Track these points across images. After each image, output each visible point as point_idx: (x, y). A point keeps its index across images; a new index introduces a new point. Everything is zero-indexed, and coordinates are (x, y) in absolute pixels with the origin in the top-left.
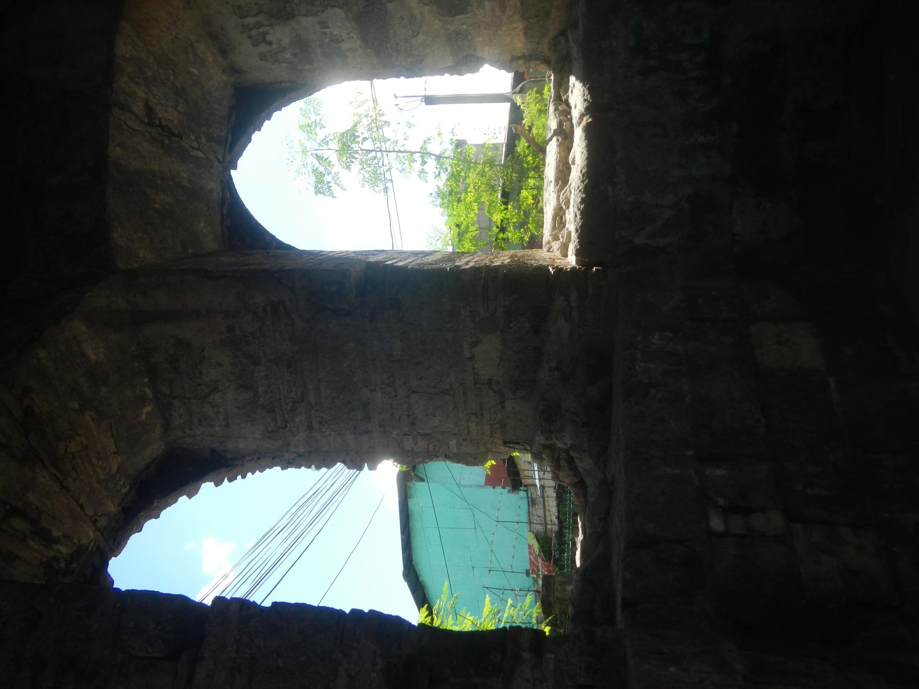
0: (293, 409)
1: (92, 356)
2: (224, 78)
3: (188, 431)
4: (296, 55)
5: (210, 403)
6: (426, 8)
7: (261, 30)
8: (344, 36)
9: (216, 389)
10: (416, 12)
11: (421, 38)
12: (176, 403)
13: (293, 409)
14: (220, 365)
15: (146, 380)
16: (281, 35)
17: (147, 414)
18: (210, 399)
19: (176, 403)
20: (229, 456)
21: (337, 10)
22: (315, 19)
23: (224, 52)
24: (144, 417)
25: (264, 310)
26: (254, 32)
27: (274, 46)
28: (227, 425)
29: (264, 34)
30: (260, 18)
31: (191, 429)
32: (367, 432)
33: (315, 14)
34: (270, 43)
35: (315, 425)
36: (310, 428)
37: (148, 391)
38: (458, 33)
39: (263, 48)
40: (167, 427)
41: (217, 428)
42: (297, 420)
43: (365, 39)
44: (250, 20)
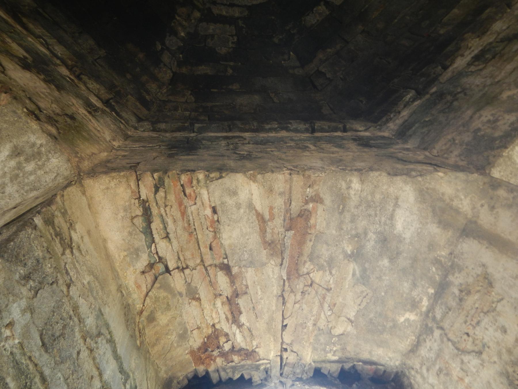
3: (424, 371)
5: (462, 362)
14: (504, 331)
15: (431, 291)
17: (408, 320)
18: (466, 358)
19: (437, 333)
24: (402, 319)
31: (428, 370)
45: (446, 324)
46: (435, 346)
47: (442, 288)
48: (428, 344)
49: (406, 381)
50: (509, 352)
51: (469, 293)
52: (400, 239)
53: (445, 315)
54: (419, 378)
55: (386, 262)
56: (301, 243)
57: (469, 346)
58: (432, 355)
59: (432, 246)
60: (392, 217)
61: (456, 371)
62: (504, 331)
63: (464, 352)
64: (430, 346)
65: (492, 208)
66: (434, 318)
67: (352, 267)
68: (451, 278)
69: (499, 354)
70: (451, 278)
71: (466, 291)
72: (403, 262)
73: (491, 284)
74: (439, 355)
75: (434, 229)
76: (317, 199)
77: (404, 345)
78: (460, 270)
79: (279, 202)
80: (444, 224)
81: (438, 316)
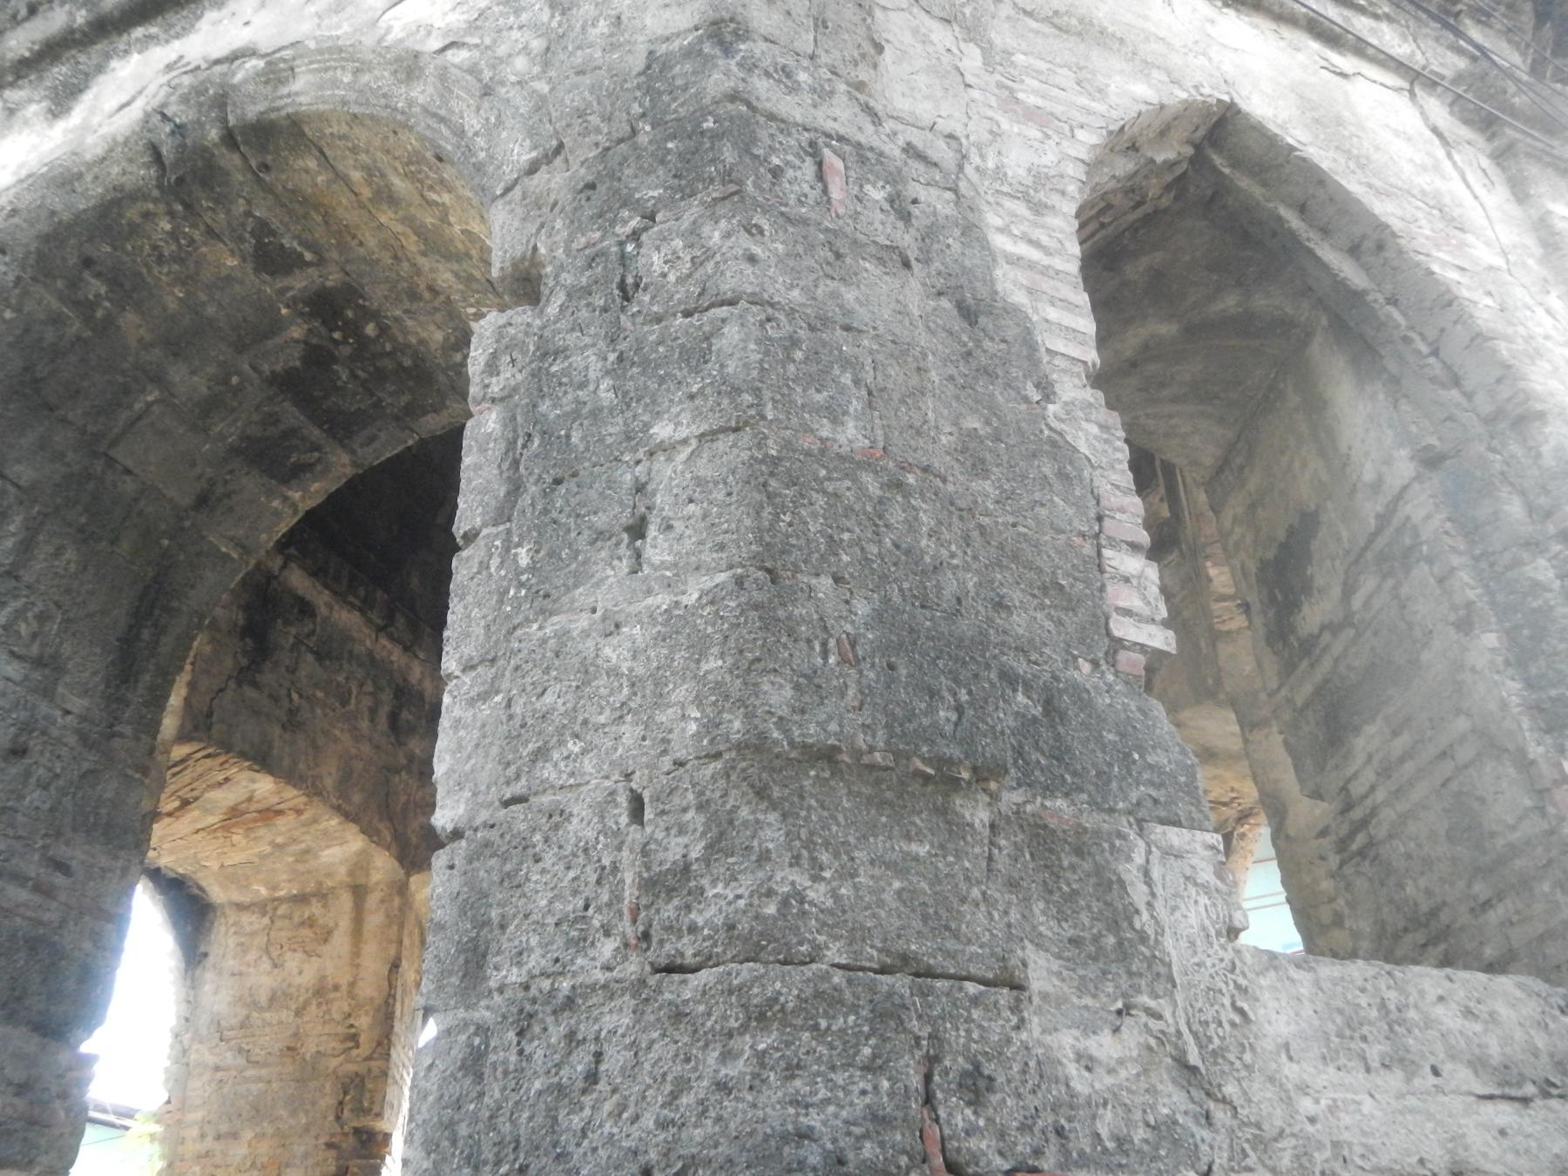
0: (240, 1050)
1: (326, 852)
3: (232, 930)
9: (275, 966)
12: (266, 920)
13: (240, 1050)
14: (300, 973)
18: (265, 958)
19: (266, 920)
20: (198, 972)
25: (352, 1026)
28: (233, 975)
32: (203, 1136)
35: (219, 1075)
36: (217, 1068)
37: (282, 893)
40: (240, 907)
41: (231, 962)
42: (229, 1055)
45: (279, 923)
46: (256, 927)
47: (301, 899)
48: (254, 918)
49: (211, 916)
50: (290, 985)
51: (311, 926)
52: (316, 857)
53: (283, 917)
54: (223, 929)
55: (291, 859)
56: (255, 821)
57: (275, 954)
58: (248, 929)
59: (328, 875)
60: (328, 847)
61: (251, 957)
62: (300, 973)
63: (268, 953)
64: (251, 921)
65: (382, 901)
66: (275, 909)
67: (268, 849)
68: (314, 901)
69: (284, 980)
70: (314, 901)
71: (310, 923)
72: (301, 867)
73: (326, 941)
74: (253, 934)
75: (343, 870)
76: (299, 812)
77: (236, 897)
78: (324, 906)
79: (276, 800)
80: (351, 873)
81: (279, 912)
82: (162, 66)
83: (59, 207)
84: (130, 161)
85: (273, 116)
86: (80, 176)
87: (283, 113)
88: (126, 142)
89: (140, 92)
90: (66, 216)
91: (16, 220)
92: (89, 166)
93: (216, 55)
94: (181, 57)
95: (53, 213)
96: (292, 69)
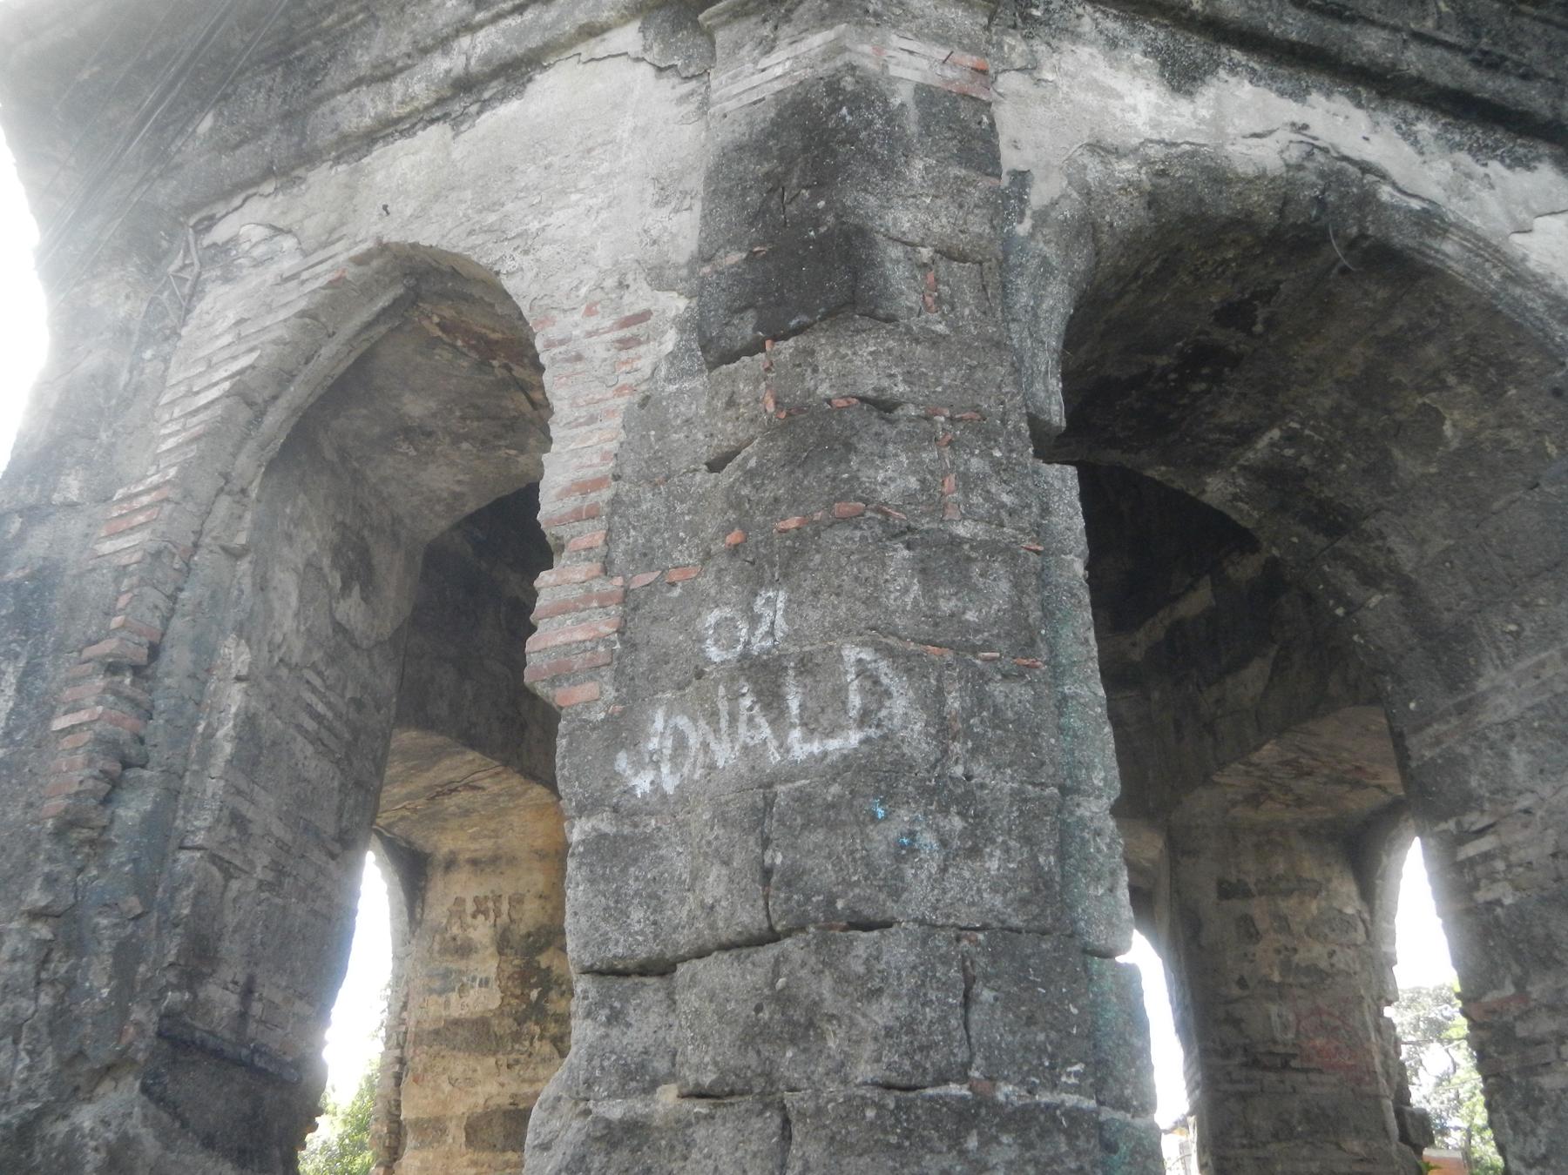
2: (445, 850)
4: (454, 939)
6: (481, 1101)
7: (492, 914)
8: (467, 1000)
10: (479, 1089)
11: (447, 1088)
16: (481, 932)
21: (498, 1003)
22: (493, 976)
23: (474, 862)
26: (490, 904)
27: (469, 920)
29: (485, 913)
30: (505, 917)
33: (498, 978)
34: (474, 916)
38: (444, 1131)
39: (470, 907)
43: (457, 1022)
44: (505, 907)
82: (1287, 119)
83: (1208, 200)
84: (1268, 197)
85: (1418, 257)
86: (1229, 182)
87: (1430, 262)
88: (1273, 180)
89: (1271, 132)
90: (1212, 212)
91: (1164, 182)
92: (1240, 179)
93: (1346, 152)
94: (1305, 127)
95: (1201, 200)
96: (1446, 231)
